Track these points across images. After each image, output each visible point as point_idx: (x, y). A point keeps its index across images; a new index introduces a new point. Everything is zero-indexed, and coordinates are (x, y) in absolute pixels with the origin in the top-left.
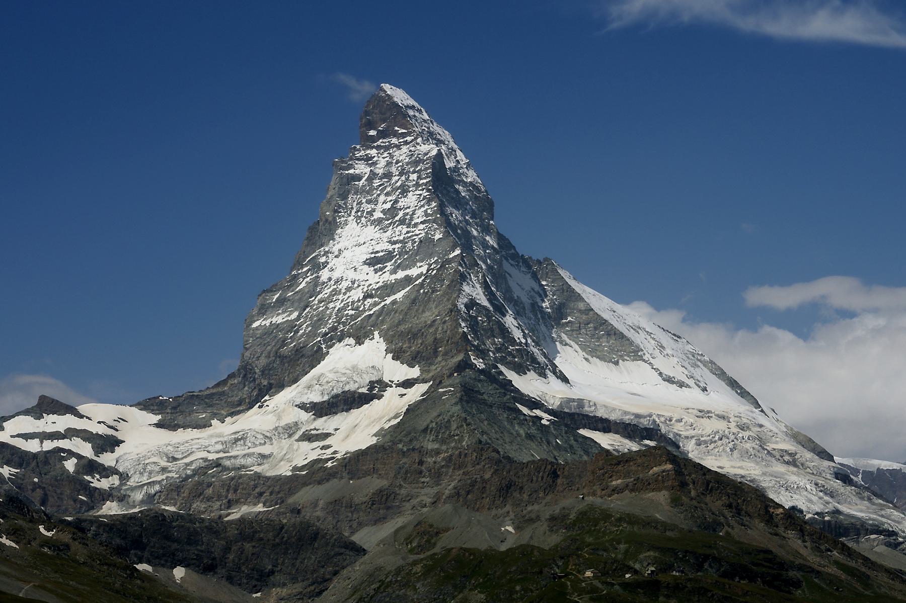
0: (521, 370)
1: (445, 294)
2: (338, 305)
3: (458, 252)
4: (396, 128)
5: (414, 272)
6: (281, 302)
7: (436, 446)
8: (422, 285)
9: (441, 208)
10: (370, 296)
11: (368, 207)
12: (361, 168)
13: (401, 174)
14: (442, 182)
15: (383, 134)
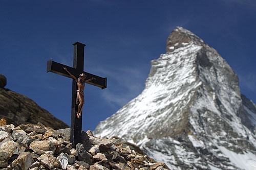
0: (238, 151)
1: (188, 105)
2: (131, 124)
3: (200, 83)
4: (183, 43)
5: (174, 101)
6: (107, 127)
8: (177, 105)
9: (197, 70)
12: (164, 63)
13: (181, 60)
14: (201, 61)
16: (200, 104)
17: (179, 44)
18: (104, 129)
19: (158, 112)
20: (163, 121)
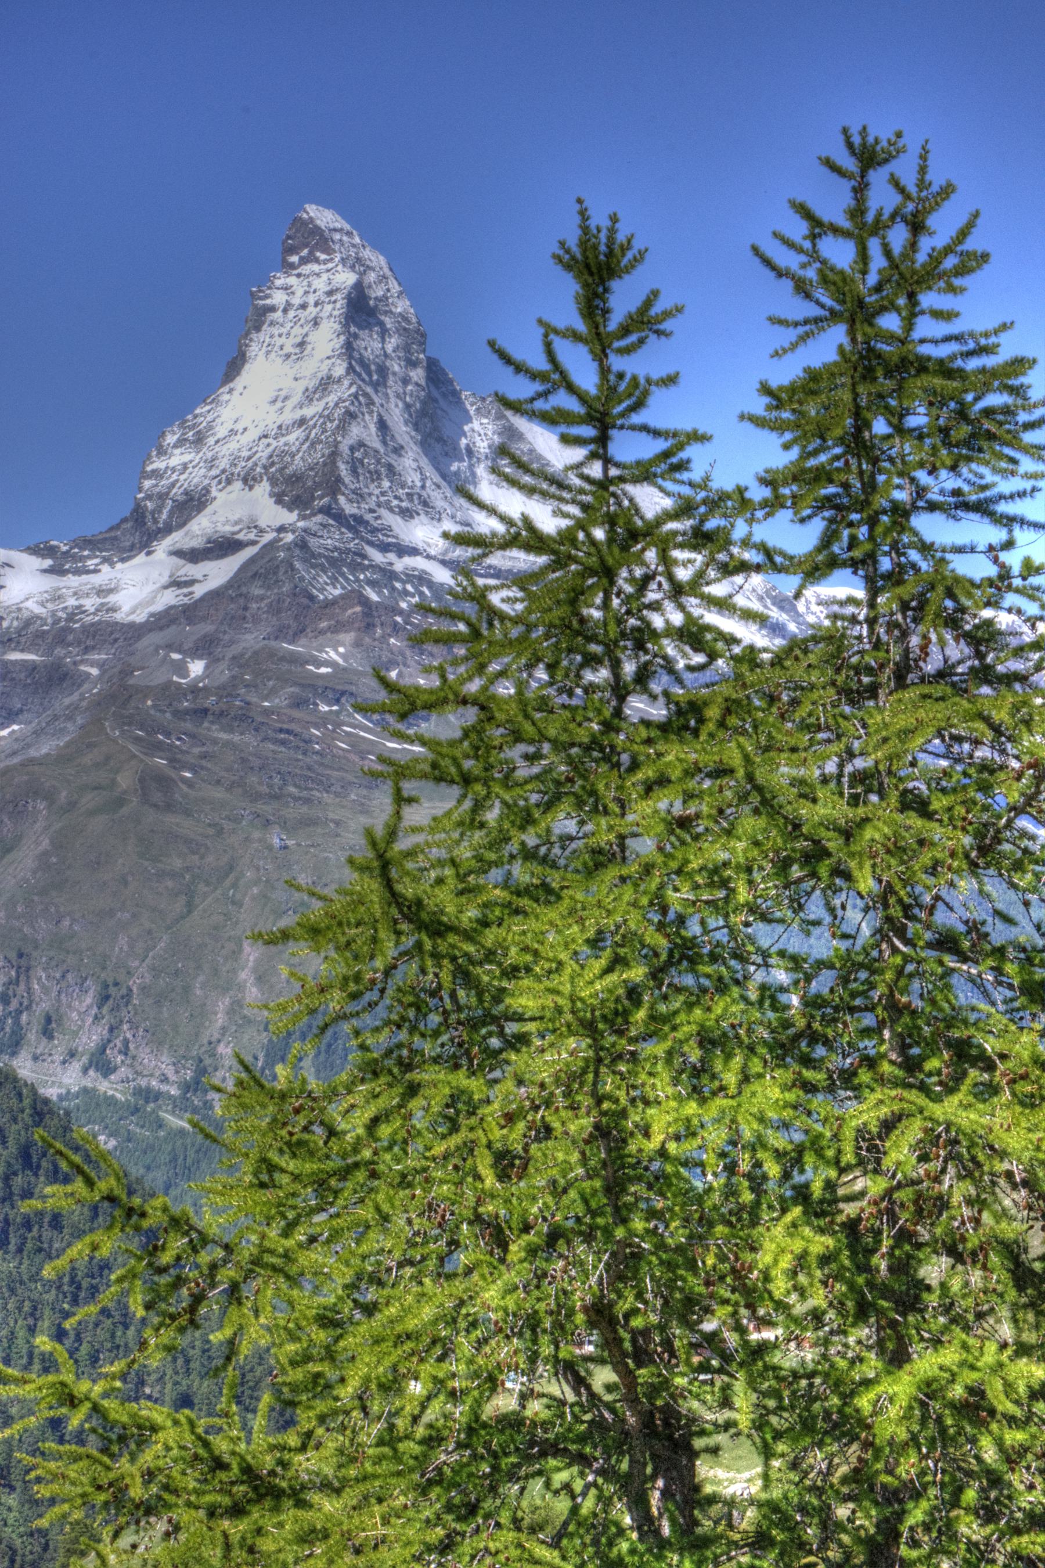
0: (407, 514)
3: (353, 389)
5: (309, 412)
6: (180, 443)
7: (261, 592)
10: (266, 436)
11: (279, 341)
13: (316, 304)
15: (304, 261)
16: (356, 431)
17: (311, 253)
18: (175, 446)
19: (282, 430)
20: (293, 456)
